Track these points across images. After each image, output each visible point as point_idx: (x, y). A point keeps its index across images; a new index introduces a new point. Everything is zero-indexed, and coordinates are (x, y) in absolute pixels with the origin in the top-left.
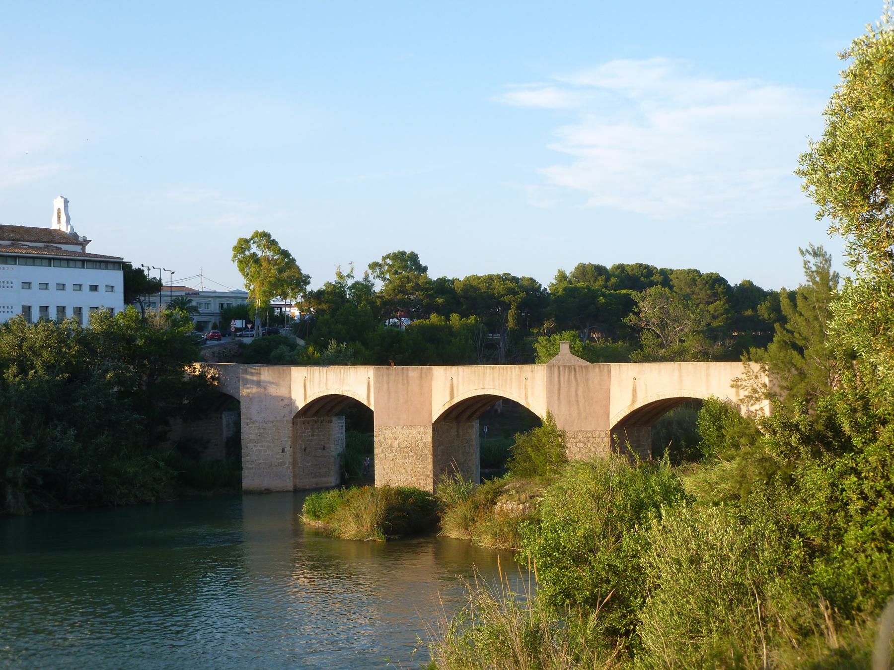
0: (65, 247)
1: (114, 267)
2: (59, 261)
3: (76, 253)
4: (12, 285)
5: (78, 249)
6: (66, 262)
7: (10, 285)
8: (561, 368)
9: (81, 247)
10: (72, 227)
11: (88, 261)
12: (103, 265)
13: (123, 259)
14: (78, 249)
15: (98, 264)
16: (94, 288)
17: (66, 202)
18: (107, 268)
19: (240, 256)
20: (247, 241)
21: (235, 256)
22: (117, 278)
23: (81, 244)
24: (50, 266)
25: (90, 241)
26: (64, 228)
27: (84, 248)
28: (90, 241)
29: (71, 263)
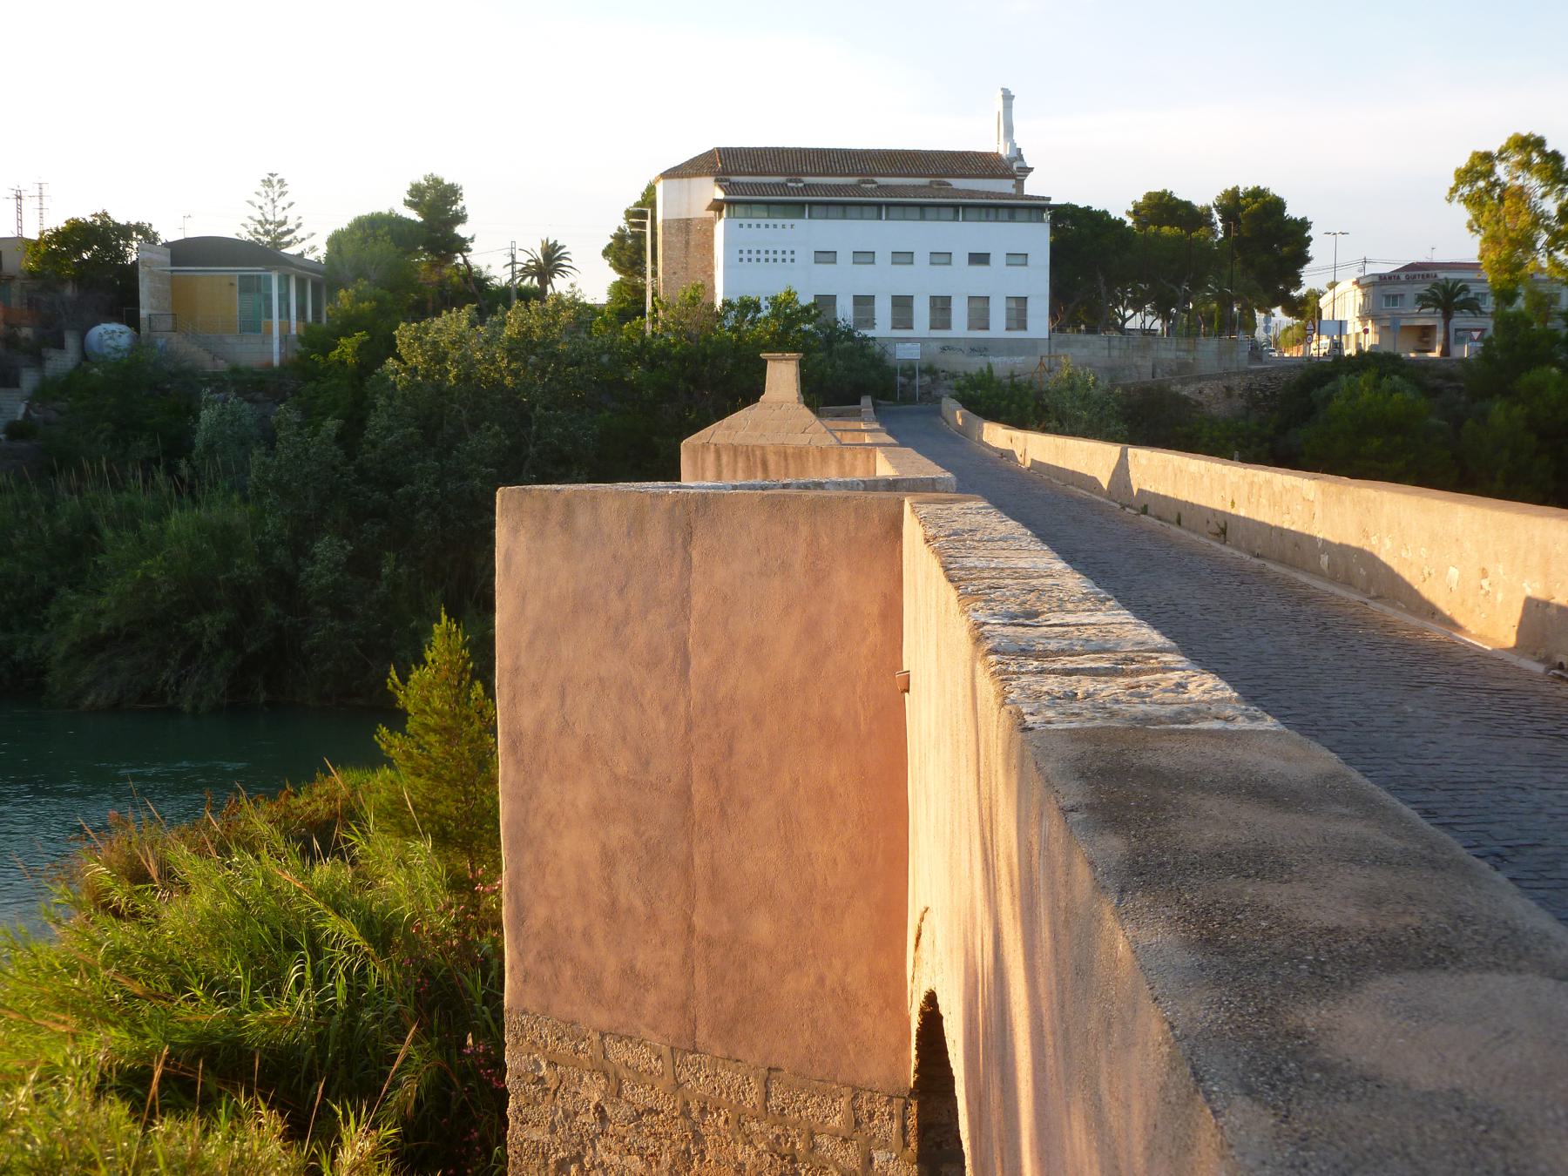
0: (958, 183)
1: (987, 216)
2: (825, 207)
3: (1010, 196)
4: (741, 256)
5: (1006, 186)
6: (917, 210)
7: (788, 257)
8: (725, 459)
9: (1013, 182)
10: (1013, 144)
11: (965, 206)
12: (1004, 213)
13: (1049, 199)
14: (1006, 186)
15: (992, 211)
16: (979, 259)
17: (1008, 97)
18: (1012, 219)
19: (1466, 190)
20: (1487, 157)
21: (1454, 190)
22: (1037, 239)
23: (1013, 176)
24: (880, 219)
25: (1031, 169)
26: (1003, 150)
27: (1020, 184)
28: (1031, 169)
29: (930, 212)
